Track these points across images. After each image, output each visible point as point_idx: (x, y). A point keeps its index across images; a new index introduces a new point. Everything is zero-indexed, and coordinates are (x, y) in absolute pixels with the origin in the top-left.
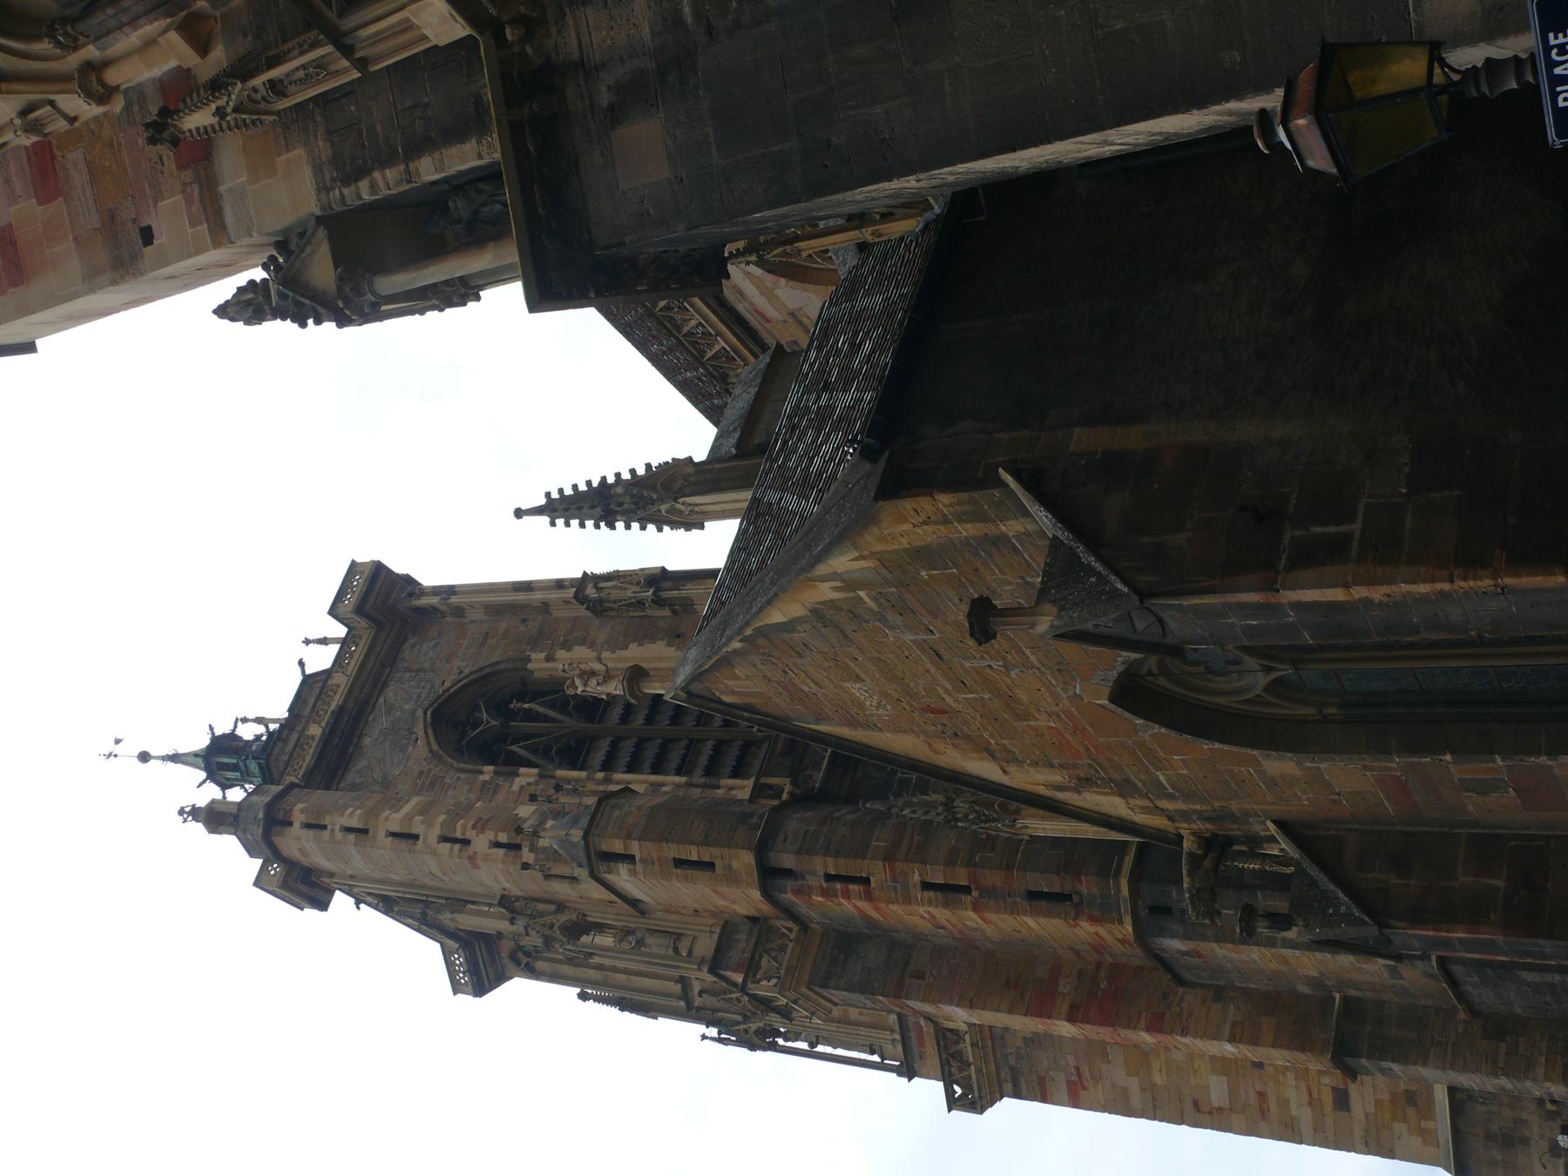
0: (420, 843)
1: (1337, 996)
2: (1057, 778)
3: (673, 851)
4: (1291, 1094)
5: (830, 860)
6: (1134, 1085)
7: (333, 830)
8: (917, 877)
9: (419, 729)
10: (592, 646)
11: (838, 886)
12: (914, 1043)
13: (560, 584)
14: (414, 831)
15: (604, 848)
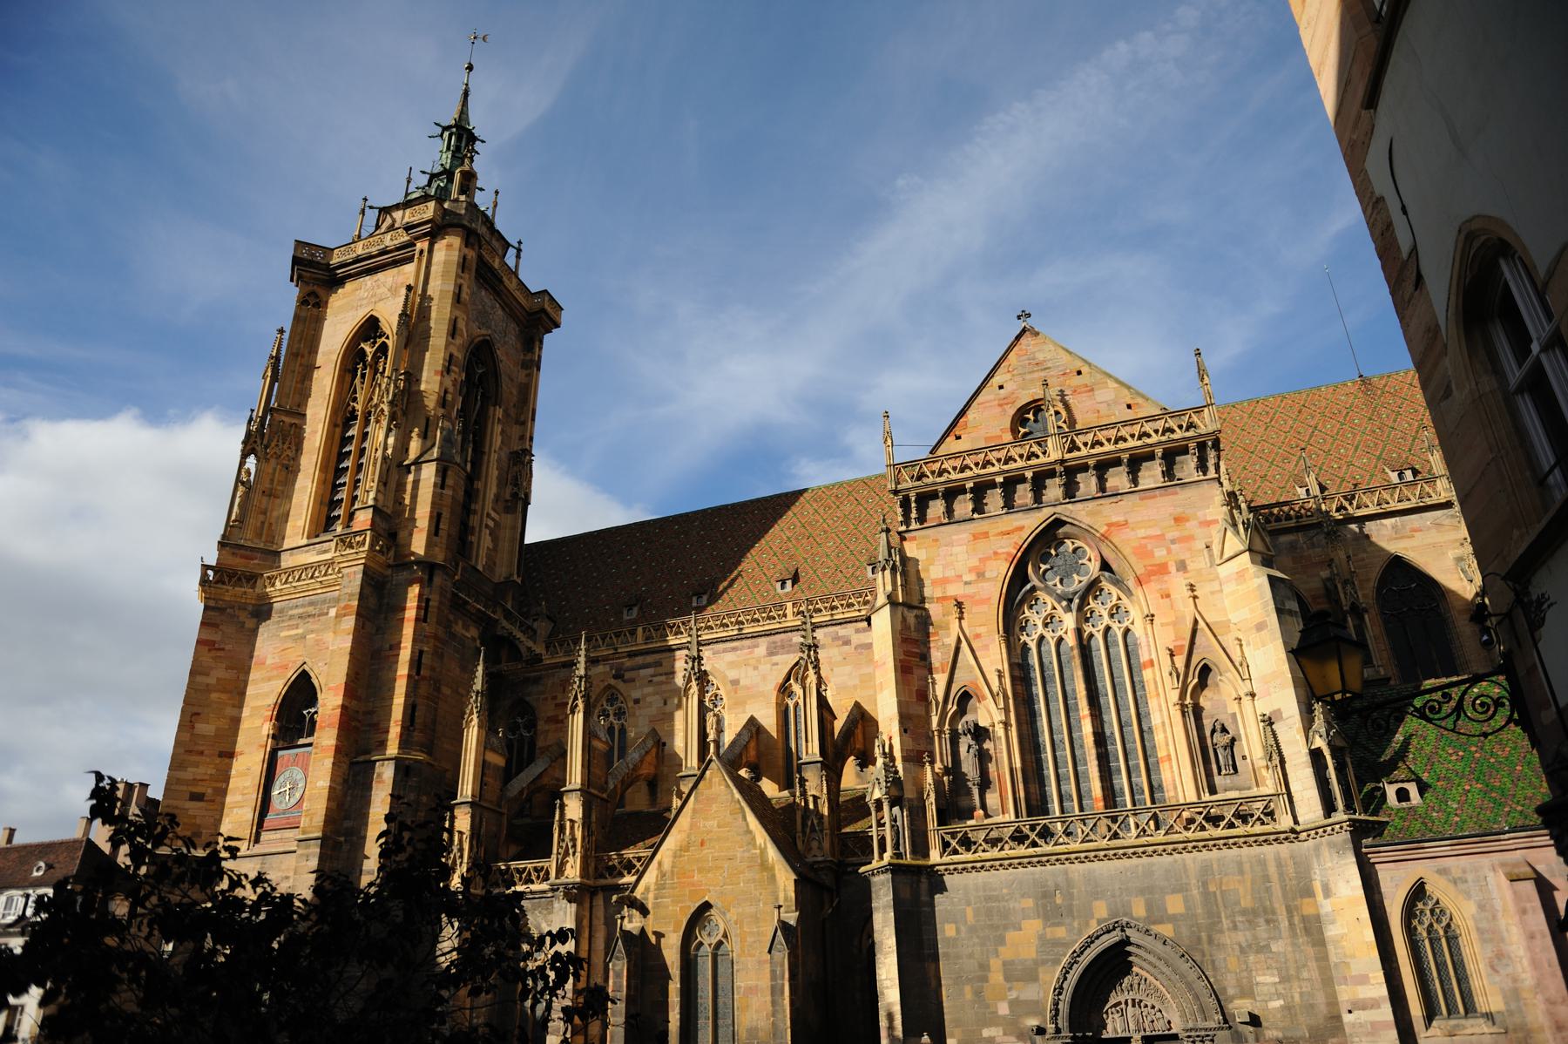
0: (450, 339)
1: (342, 839)
2: (667, 866)
3: (446, 514)
4: (201, 770)
5: (436, 604)
6: (212, 680)
7: (461, 278)
8: (426, 649)
9: (484, 332)
10: (500, 448)
11: (424, 604)
12: (242, 552)
13: (531, 439)
14: (457, 337)
15: (449, 473)
